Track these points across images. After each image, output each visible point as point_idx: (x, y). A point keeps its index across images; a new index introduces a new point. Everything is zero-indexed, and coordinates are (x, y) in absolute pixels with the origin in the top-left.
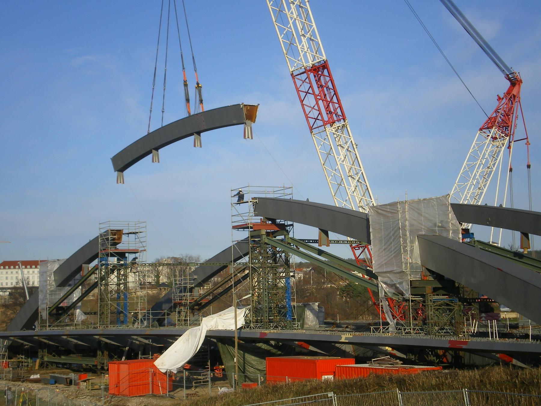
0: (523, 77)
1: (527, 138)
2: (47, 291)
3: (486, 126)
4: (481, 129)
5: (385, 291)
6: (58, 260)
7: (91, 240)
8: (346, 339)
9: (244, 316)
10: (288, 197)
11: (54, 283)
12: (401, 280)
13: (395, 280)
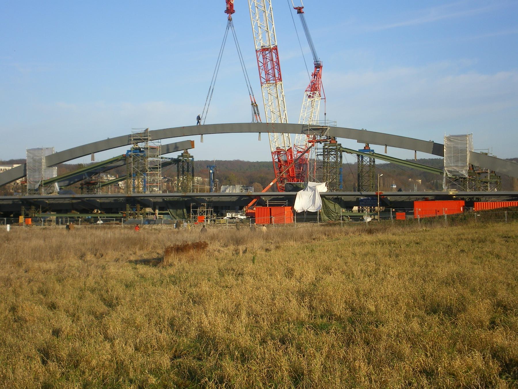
0: (323, 64)
1: (325, 99)
2: (41, 169)
3: (310, 90)
4: (306, 91)
5: (446, 174)
6: (47, 148)
7: (110, 138)
8: (453, 193)
9: (326, 186)
10: (336, 126)
11: (45, 164)
12: (462, 170)
13: (457, 169)
